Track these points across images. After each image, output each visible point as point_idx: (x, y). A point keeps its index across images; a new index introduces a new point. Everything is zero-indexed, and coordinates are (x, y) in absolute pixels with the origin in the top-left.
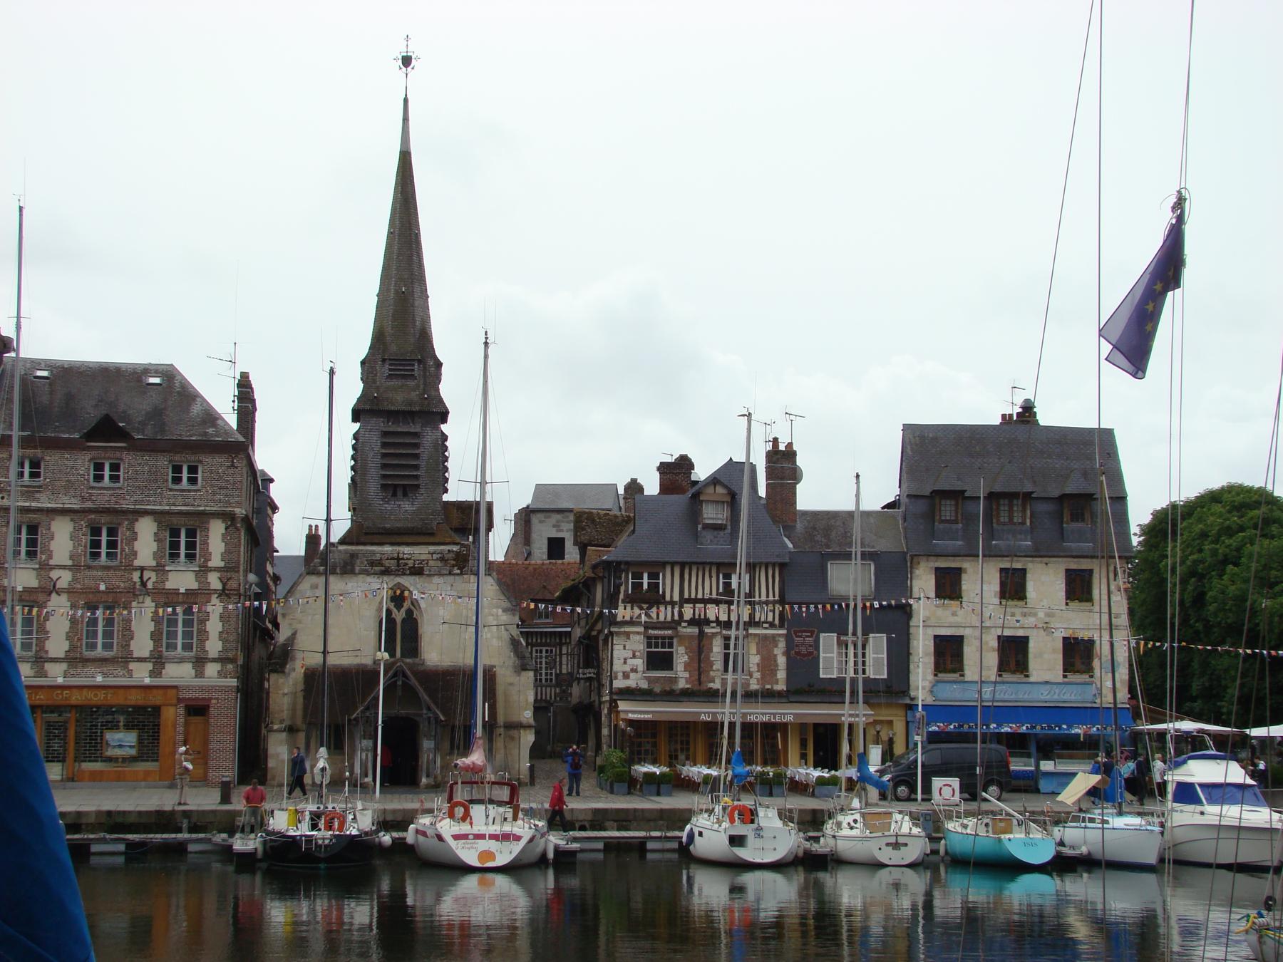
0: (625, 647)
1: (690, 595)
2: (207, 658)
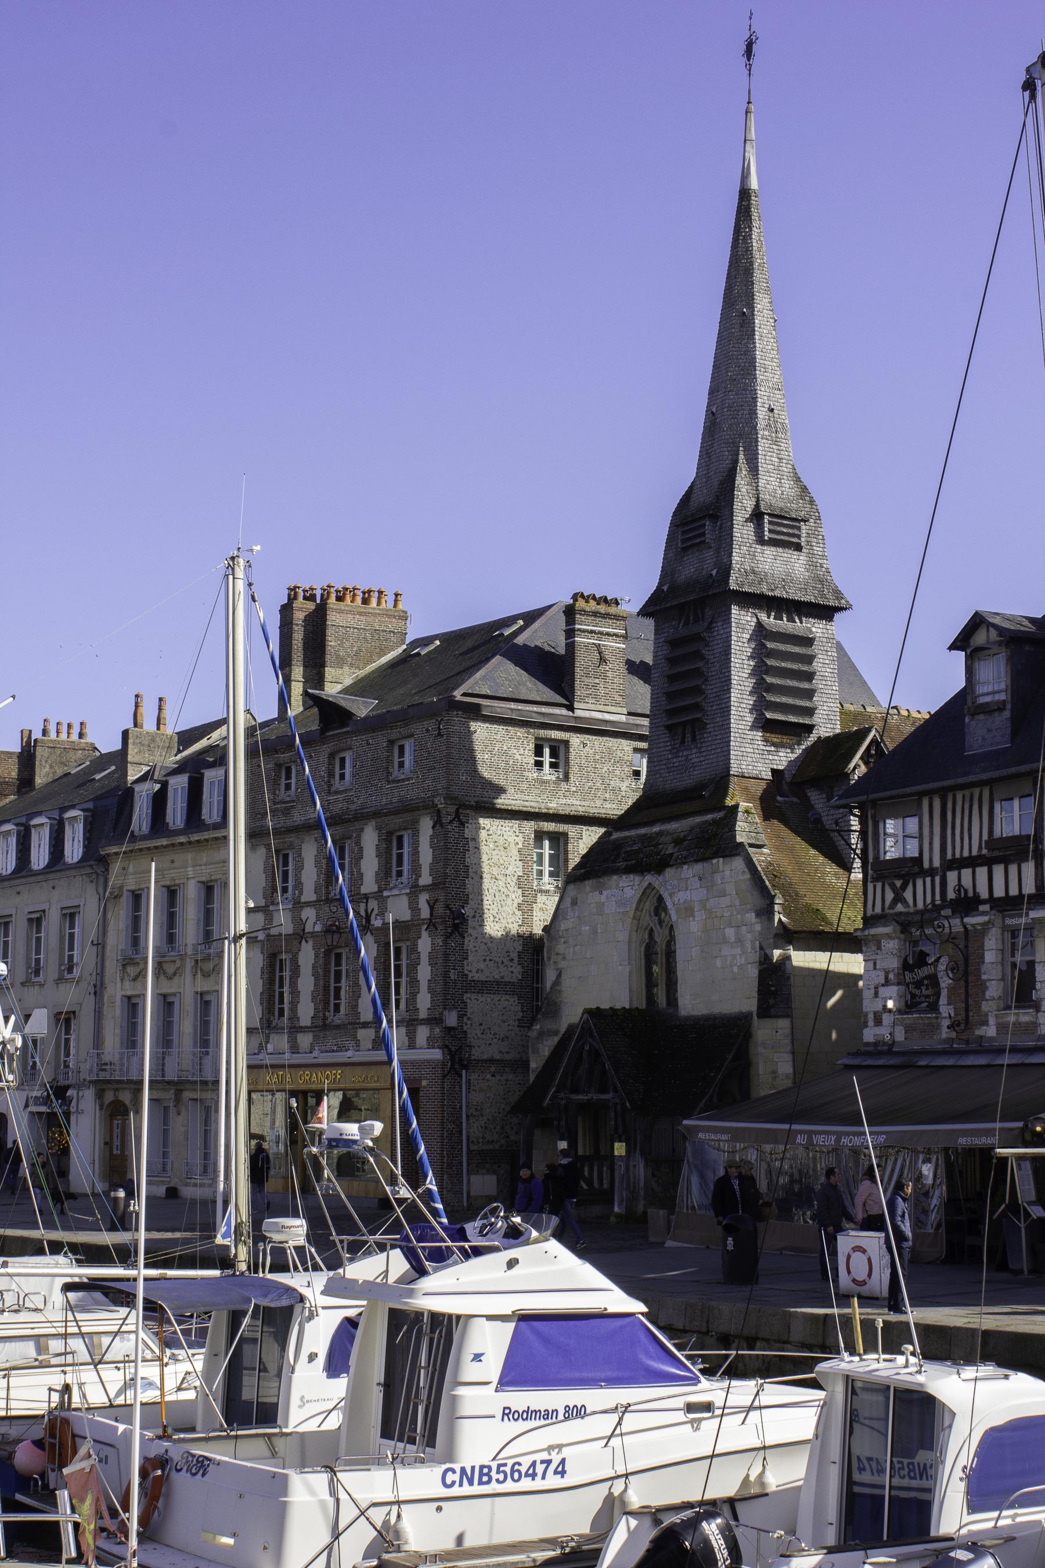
0: (875, 964)
1: (954, 854)
2: (417, 1020)
